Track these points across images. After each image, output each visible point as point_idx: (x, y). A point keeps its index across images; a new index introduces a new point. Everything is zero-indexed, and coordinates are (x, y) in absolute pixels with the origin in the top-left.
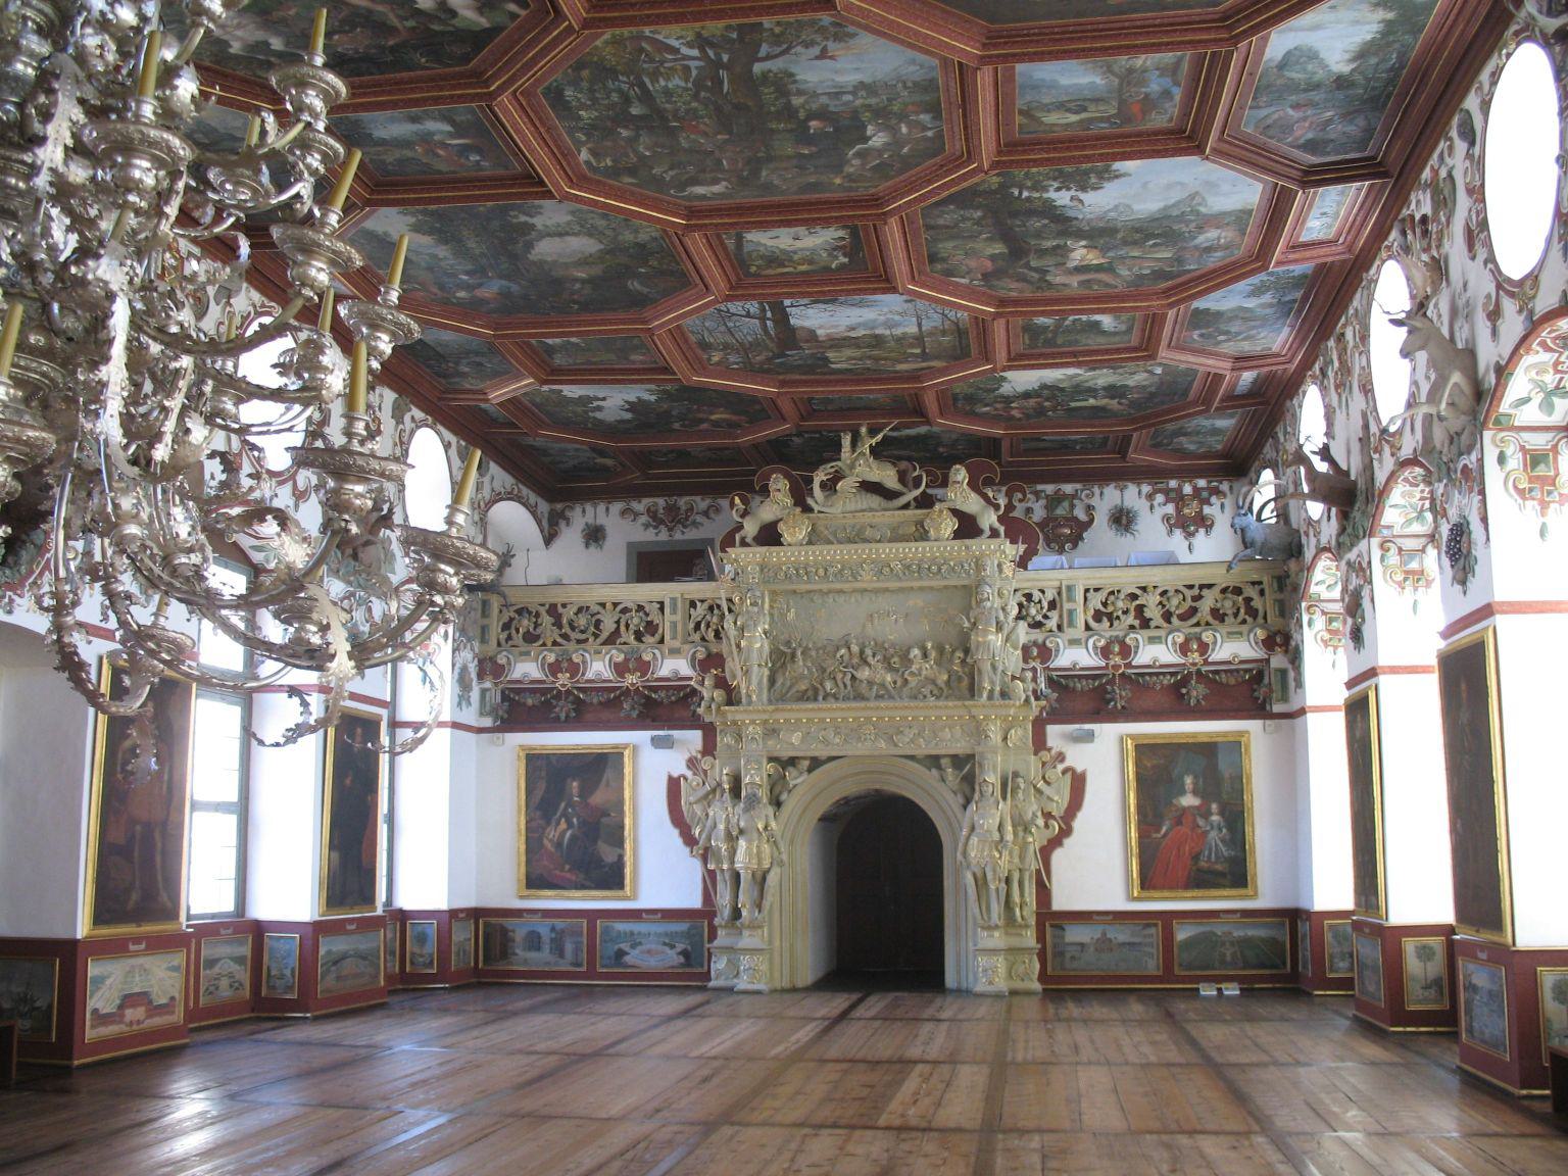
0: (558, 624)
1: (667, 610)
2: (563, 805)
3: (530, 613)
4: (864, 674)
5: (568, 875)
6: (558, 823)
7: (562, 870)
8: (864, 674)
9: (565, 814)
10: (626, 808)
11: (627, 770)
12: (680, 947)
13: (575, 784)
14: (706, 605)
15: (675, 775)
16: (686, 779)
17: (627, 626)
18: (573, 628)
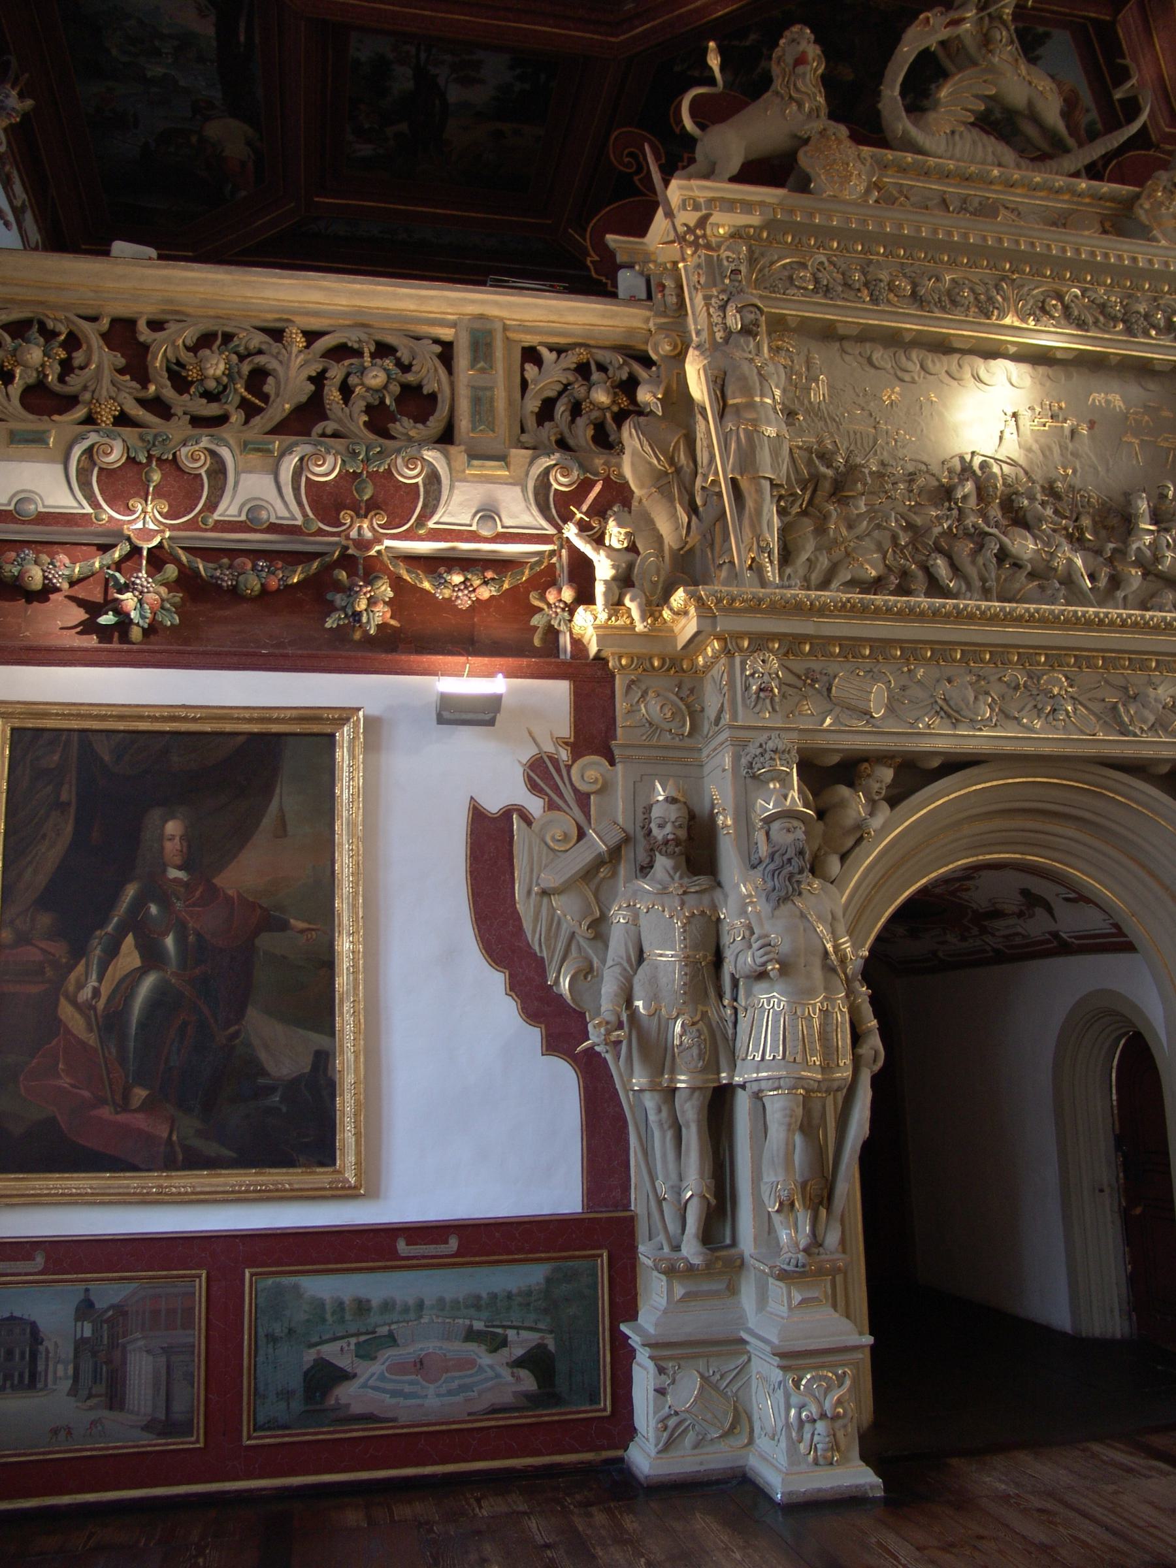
0: (137, 368)
1: (462, 360)
2: (131, 891)
3: (49, 335)
4: (1026, 546)
5: (140, 1121)
6: (112, 951)
7: (124, 1105)
8: (1026, 546)
9: (135, 923)
10: (342, 905)
11: (346, 789)
12: (521, 1342)
13: (172, 827)
14: (571, 360)
15: (493, 805)
16: (527, 819)
17: (346, 390)
18: (180, 383)
